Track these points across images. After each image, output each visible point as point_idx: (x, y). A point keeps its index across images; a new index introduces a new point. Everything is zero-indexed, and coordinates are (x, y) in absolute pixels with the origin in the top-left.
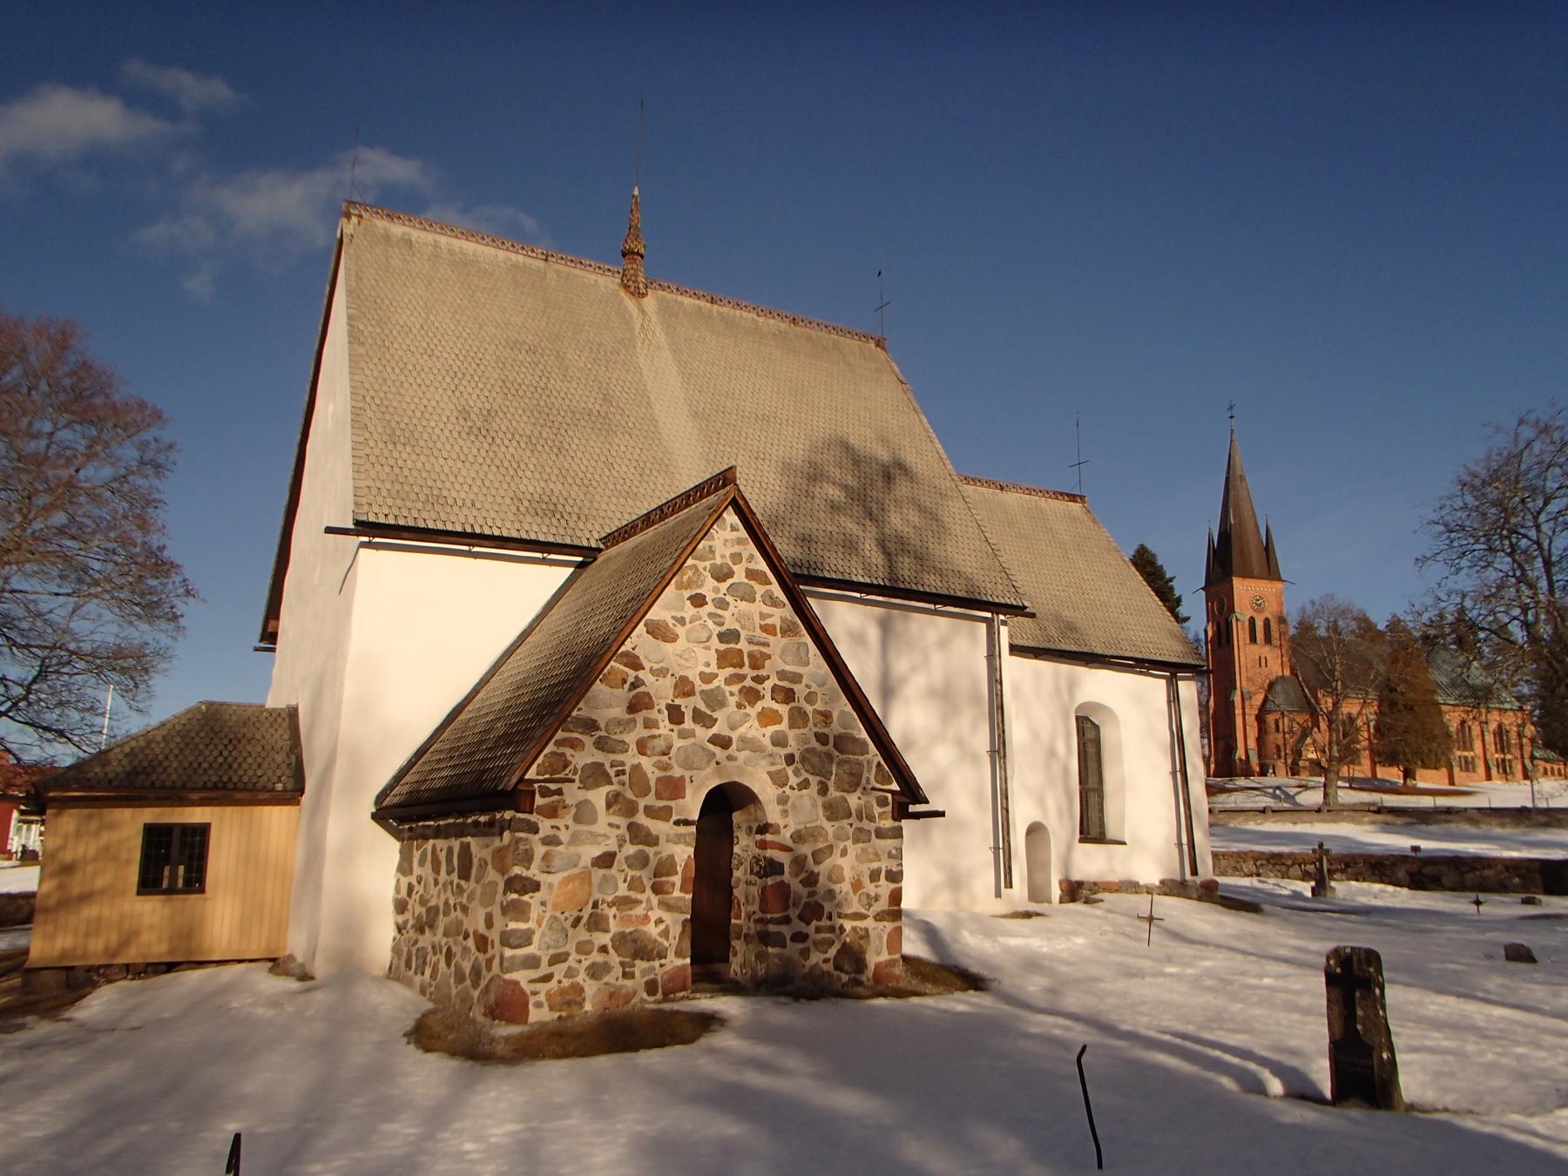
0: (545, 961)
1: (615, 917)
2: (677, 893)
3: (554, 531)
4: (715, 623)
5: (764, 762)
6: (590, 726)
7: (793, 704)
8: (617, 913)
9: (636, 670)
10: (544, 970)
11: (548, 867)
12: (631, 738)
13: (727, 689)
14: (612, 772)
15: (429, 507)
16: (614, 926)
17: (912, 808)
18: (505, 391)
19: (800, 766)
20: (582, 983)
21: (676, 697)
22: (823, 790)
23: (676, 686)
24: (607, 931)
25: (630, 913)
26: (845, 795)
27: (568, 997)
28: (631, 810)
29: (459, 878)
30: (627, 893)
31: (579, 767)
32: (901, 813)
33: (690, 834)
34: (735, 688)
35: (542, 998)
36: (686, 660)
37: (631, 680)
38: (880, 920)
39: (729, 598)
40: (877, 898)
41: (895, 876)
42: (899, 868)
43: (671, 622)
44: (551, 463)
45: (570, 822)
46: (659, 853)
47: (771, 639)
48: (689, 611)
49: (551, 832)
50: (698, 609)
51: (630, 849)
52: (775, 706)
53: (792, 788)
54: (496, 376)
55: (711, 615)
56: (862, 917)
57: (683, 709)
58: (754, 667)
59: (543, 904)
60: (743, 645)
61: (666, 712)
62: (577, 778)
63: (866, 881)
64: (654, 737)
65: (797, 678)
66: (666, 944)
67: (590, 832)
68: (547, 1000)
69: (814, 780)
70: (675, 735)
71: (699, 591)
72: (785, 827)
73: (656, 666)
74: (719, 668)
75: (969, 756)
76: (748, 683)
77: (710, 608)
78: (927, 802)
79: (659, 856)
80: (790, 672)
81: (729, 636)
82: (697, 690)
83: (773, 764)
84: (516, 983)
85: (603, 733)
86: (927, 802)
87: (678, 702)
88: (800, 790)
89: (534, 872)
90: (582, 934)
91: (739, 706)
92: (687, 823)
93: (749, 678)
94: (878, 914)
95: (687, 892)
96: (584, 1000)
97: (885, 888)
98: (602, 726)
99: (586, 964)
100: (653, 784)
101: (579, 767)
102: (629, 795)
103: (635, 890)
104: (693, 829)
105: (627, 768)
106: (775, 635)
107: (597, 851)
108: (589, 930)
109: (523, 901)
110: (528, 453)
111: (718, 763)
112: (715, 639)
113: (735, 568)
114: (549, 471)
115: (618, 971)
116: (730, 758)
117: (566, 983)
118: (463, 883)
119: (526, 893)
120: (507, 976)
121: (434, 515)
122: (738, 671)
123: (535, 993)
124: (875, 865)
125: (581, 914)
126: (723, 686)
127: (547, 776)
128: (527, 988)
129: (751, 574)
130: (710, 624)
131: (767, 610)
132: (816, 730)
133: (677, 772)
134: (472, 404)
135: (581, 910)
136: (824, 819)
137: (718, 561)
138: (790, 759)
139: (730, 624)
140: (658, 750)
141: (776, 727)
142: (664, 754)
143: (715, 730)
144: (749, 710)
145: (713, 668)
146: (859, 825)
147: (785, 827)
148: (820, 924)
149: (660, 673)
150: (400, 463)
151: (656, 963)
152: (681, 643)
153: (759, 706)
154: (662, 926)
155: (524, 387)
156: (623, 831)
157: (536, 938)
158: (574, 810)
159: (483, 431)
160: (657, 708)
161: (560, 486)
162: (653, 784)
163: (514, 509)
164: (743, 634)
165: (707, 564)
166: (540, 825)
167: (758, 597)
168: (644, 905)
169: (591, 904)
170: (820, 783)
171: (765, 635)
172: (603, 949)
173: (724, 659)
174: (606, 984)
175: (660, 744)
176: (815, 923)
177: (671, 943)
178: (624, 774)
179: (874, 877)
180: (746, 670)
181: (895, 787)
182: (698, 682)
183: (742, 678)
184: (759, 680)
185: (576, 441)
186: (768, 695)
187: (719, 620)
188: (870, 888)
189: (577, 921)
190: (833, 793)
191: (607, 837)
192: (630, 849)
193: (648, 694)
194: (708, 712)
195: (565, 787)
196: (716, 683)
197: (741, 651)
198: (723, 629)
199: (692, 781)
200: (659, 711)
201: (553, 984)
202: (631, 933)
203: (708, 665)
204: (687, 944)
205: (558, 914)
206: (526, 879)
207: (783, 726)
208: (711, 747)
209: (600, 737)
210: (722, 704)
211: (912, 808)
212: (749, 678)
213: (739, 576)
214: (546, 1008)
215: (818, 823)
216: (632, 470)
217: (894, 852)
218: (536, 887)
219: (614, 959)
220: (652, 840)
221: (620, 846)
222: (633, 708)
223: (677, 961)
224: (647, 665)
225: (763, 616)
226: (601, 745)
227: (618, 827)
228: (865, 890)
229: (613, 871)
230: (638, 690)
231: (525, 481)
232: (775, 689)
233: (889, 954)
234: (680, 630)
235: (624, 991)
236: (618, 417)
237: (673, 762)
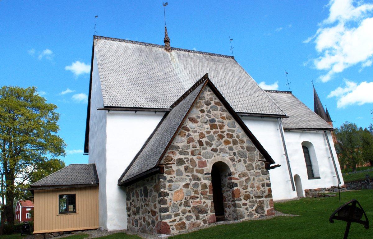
0: (173, 216)
1: (191, 202)
2: (208, 194)
3: (157, 105)
4: (208, 117)
5: (227, 155)
6: (177, 148)
7: (233, 138)
8: (192, 201)
9: (188, 131)
10: (173, 218)
11: (170, 188)
12: (189, 151)
13: (214, 135)
14: (185, 160)
15: (123, 102)
16: (192, 205)
17: (271, 165)
18: (140, 74)
19: (238, 156)
20: (185, 222)
21: (201, 138)
22: (245, 162)
23: (200, 135)
24: (189, 206)
25: (196, 201)
26: (252, 163)
27: (181, 226)
28: (192, 171)
29: (144, 197)
30: (194, 195)
31: (176, 160)
32: (268, 168)
33: (210, 177)
34: (217, 135)
35: (174, 227)
36: (202, 128)
37: (187, 134)
38: (267, 198)
39: (211, 110)
40: (265, 192)
41: (269, 185)
42: (269, 183)
43: (196, 118)
44: (154, 90)
45: (175, 175)
46: (202, 183)
47: (224, 121)
48: (200, 114)
49: (170, 179)
50: (203, 114)
51: (193, 182)
52: (228, 139)
53: (236, 162)
54: (137, 71)
55: (207, 115)
56: (262, 197)
57: (203, 141)
59: (170, 199)
61: (198, 143)
62: (175, 163)
63: (261, 187)
64: (196, 150)
65: (233, 131)
66: (207, 209)
67: (181, 178)
68: (175, 227)
70: (201, 149)
71: (202, 109)
72: (236, 173)
73: (193, 130)
74: (211, 129)
76: (220, 133)
77: (206, 113)
78: (274, 163)
79: (202, 184)
80: (231, 130)
81: (213, 121)
82: (206, 136)
83: (230, 155)
84: (166, 223)
85: (181, 150)
86: (274, 163)
87: (201, 140)
88: (239, 162)
89: (166, 190)
90: (183, 208)
91: (218, 140)
92: (208, 174)
93: (220, 132)
94: (266, 196)
95: (211, 194)
96: (186, 226)
97: (267, 188)
98: (181, 147)
99: (185, 216)
100: (197, 163)
101: (176, 160)
102: (191, 167)
103: (196, 194)
104: (210, 175)
105: (189, 159)
106: (225, 119)
107: (184, 183)
108: (185, 206)
109: (165, 199)
110: (148, 88)
111: (215, 156)
112: (209, 122)
113: (211, 102)
114: (154, 91)
115: (195, 217)
116: (218, 155)
117: (180, 222)
118: (146, 198)
119: (165, 196)
120: (163, 221)
121: (125, 104)
122: (216, 130)
123: (171, 225)
124: (262, 182)
125: (182, 202)
126: (213, 134)
127: (167, 163)
128: (169, 224)
129: (216, 103)
130: (207, 117)
131: (222, 113)
132: (241, 145)
133: (204, 159)
134: (131, 78)
135: (181, 201)
136: (247, 170)
137: (206, 100)
138: (235, 154)
139: (212, 117)
140: (197, 153)
141: (229, 145)
142: (199, 155)
143: (212, 147)
144: (221, 141)
145: (209, 130)
146: (257, 171)
147: (236, 173)
148: (250, 200)
149: (195, 132)
150: (115, 92)
151: (205, 215)
152: (199, 124)
153: (224, 139)
154: (205, 204)
155: (144, 73)
156: (191, 177)
157: (170, 210)
158: (176, 172)
159: (135, 84)
160: (195, 142)
161: (157, 95)
162: (197, 163)
163: (146, 101)
164: (216, 119)
165: (204, 101)
166: (167, 177)
167: (219, 110)
168: (199, 198)
169: (184, 198)
170: (244, 160)
171: (222, 120)
172: (189, 211)
174: (192, 221)
175: (198, 152)
176: (248, 200)
177: (209, 208)
178: (189, 161)
179: (263, 186)
180: (218, 130)
181: (265, 160)
182: (206, 134)
183: (218, 132)
184: (223, 132)
185: (160, 84)
186: (226, 136)
187: (209, 116)
189: (181, 204)
190: (248, 162)
191: (186, 179)
192: (193, 182)
193: (192, 138)
194: (210, 142)
195: (172, 165)
196: (211, 134)
197: (216, 124)
198: (211, 119)
199: (208, 162)
200: (196, 142)
201: (176, 222)
202: (197, 206)
203: (208, 129)
204: (213, 208)
205: (175, 202)
206: (165, 192)
207: (231, 145)
208: (212, 152)
209: (180, 151)
210: (214, 140)
211: (271, 165)
212: (220, 132)
213: (213, 103)
214: (175, 230)
215: (245, 171)
216: (175, 90)
217: (267, 178)
218: (168, 194)
219: (192, 214)
220: (199, 179)
221: (190, 181)
222: (189, 142)
223: (211, 214)
224: (190, 129)
225: (221, 114)
226: (181, 153)
227: (189, 176)
228: (261, 189)
229: (189, 189)
230: (189, 137)
231: (148, 94)
232: (227, 134)
233: (271, 207)
234: (199, 120)
235: (197, 223)
236: (170, 78)
237: (202, 157)
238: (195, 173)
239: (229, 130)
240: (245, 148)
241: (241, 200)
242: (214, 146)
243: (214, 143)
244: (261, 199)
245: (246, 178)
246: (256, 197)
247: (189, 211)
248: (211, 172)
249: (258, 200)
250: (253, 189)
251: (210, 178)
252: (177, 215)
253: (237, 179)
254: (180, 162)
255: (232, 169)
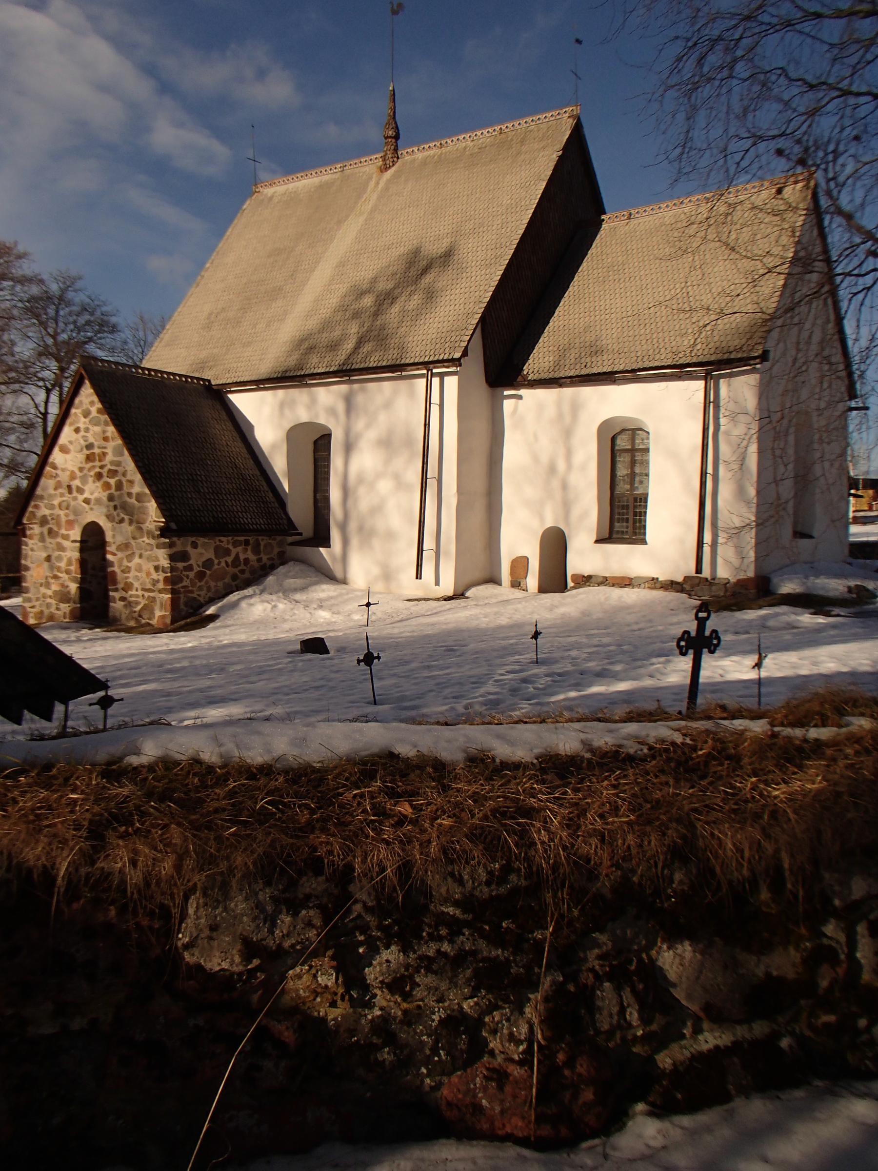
14: (49, 518)
24: (49, 589)
43: (68, 444)
56: (153, 591)
58: (100, 461)
60: (96, 450)
69: (126, 517)
75: (400, 484)
81: (89, 446)
104: (78, 544)
115: (54, 607)
124: (156, 564)
172: (50, 597)
173: (89, 458)
186: (105, 474)
188: (155, 576)
234: (71, 447)
238: (59, 540)
239: (112, 463)
240: (134, 495)
241: (116, 590)
242: (86, 495)
243: (86, 488)
244: (152, 594)
245: (130, 552)
246: (143, 589)
247: (50, 597)
248: (79, 539)
249: (146, 594)
250: (139, 574)
251: (78, 549)
252: (38, 599)
253: (114, 554)
254: (44, 521)
255: (109, 538)
